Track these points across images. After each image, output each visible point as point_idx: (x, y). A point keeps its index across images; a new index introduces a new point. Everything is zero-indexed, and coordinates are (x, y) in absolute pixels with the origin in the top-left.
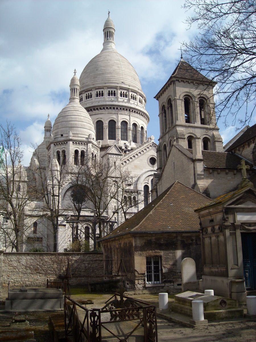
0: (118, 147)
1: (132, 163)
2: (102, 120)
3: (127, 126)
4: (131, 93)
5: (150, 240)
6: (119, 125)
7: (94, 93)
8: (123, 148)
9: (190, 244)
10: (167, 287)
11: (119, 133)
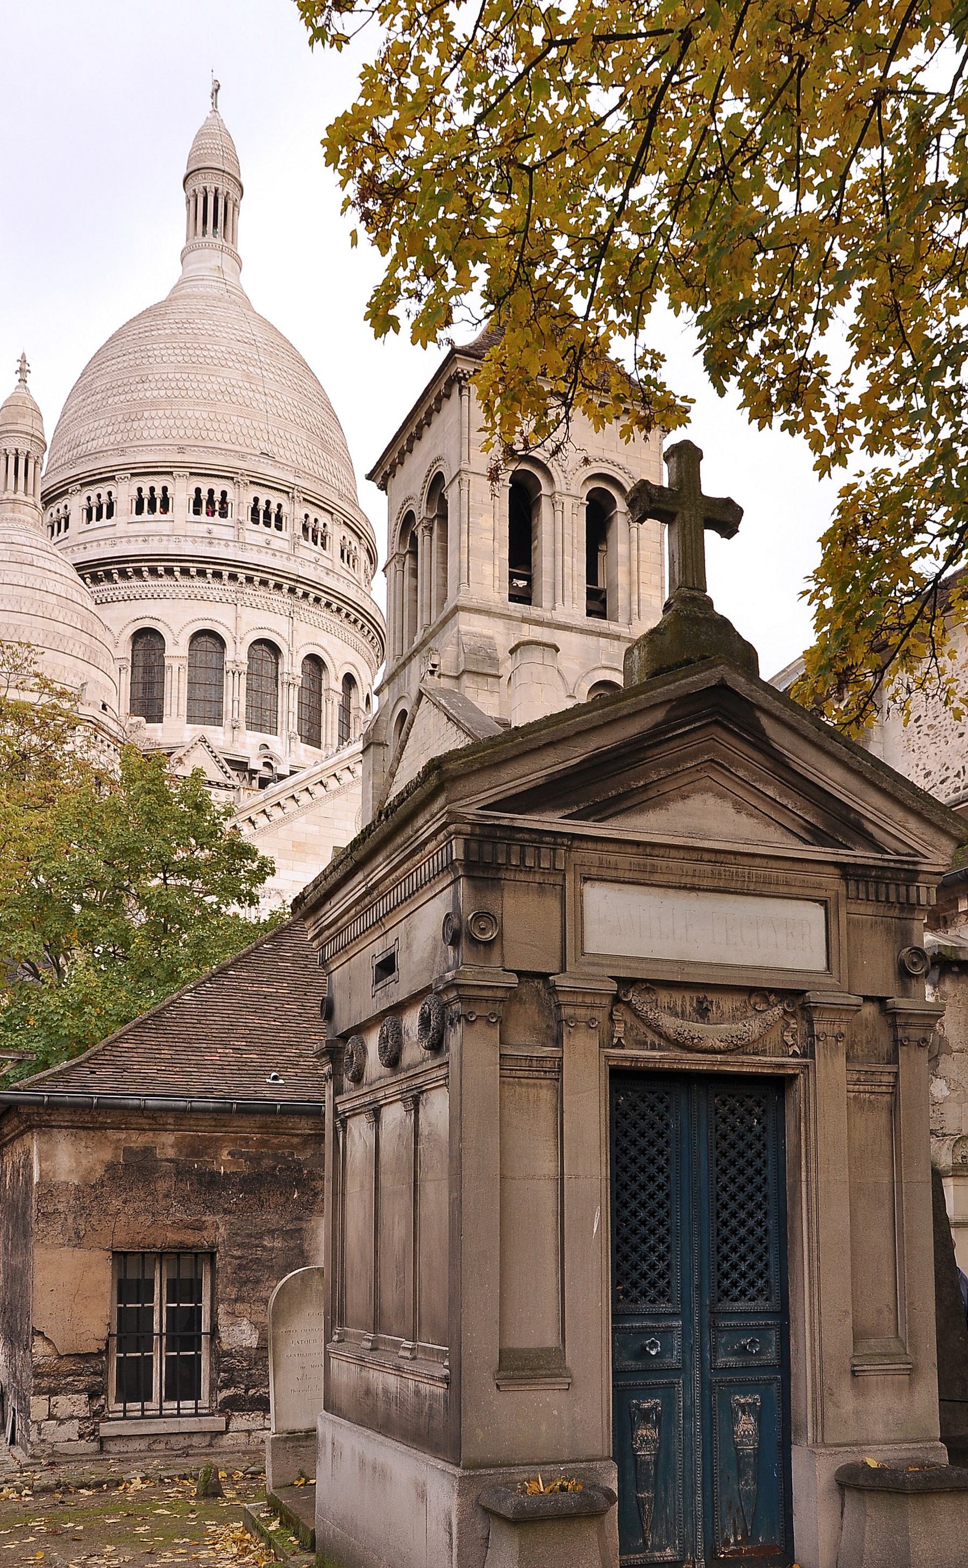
0: (221, 757)
1: (282, 832)
2: (159, 627)
3: (277, 664)
4: (301, 510)
5: (148, 1151)
7: (124, 493)
8: (256, 764)
10: (242, 1438)
11: (235, 695)
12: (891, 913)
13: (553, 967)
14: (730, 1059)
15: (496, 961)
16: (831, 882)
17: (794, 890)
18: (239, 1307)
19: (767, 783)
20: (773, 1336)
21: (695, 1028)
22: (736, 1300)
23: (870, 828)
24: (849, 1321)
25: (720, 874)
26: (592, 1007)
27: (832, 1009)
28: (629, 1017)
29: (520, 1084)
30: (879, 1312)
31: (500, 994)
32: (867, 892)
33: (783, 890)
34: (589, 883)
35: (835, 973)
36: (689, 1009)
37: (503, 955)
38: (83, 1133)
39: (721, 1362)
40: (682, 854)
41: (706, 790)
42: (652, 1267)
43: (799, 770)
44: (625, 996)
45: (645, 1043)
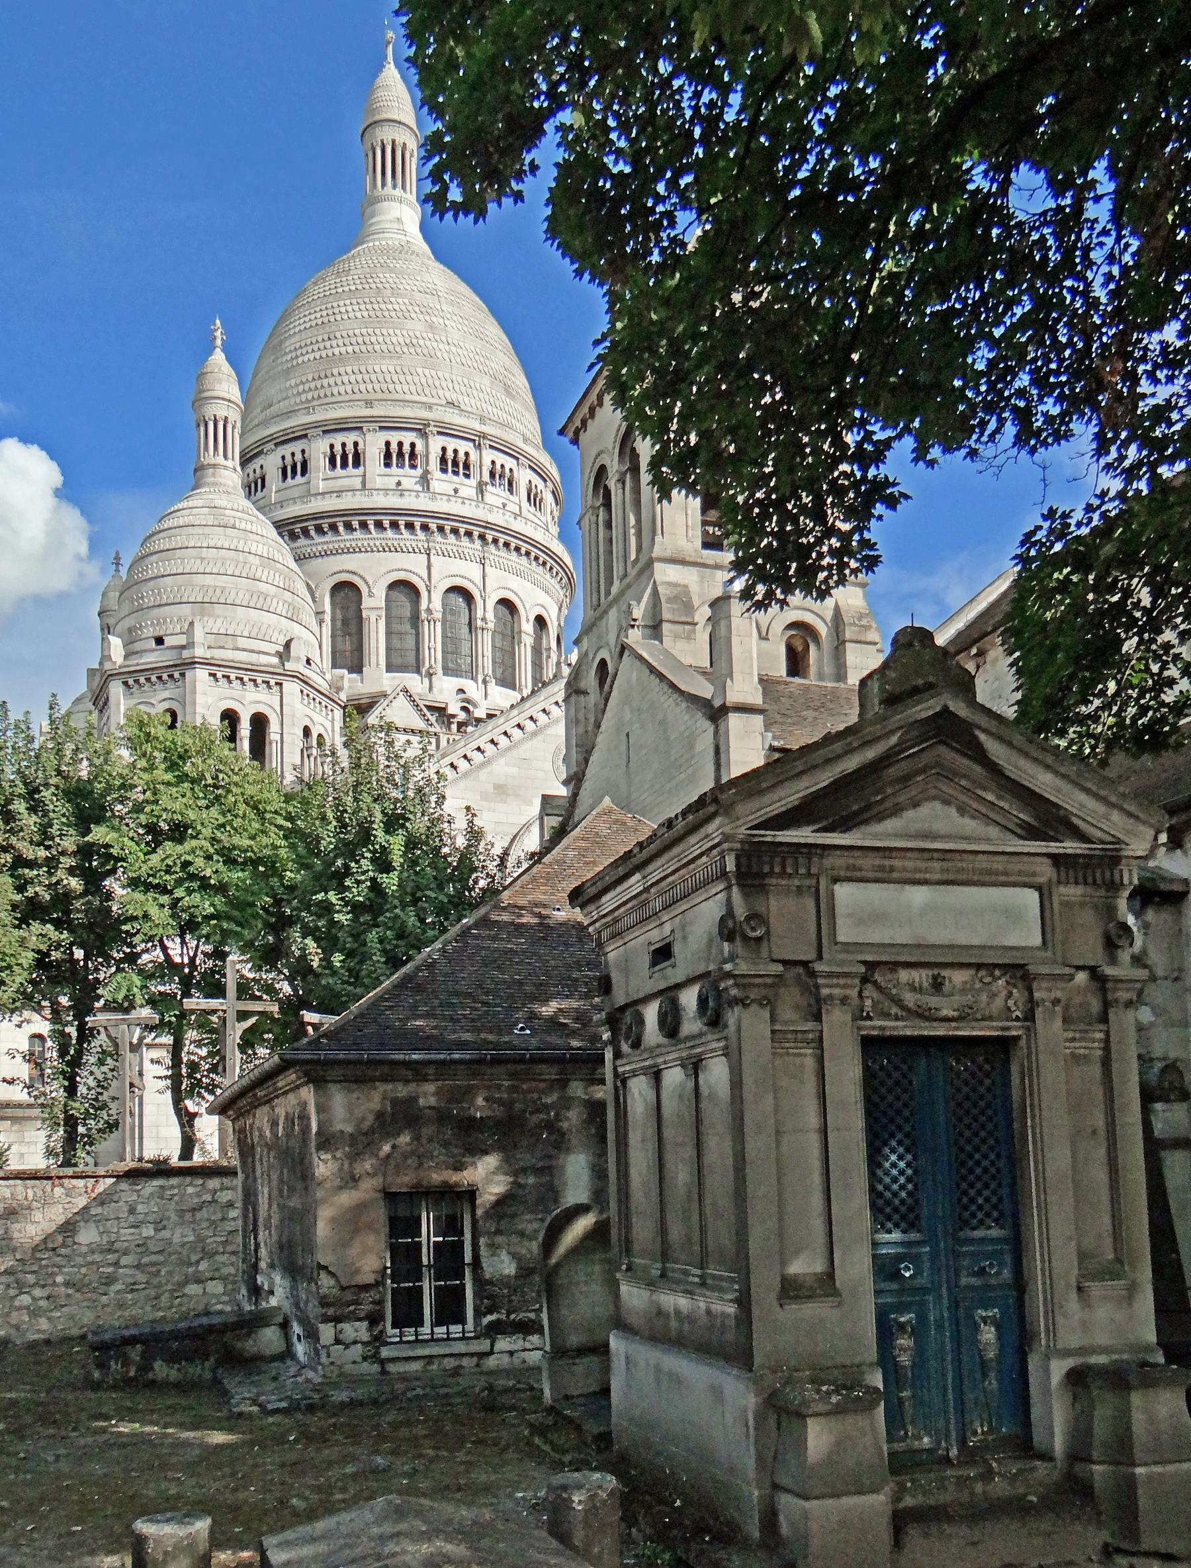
4: (489, 456)
5: (412, 1100)
6: (433, 602)
7: (319, 449)
10: (506, 1359)
13: (811, 955)
15: (765, 954)
16: (1046, 871)
17: (1012, 879)
18: (499, 1239)
19: (985, 789)
20: (1008, 1258)
21: (933, 1001)
23: (1075, 821)
26: (844, 987)
28: (875, 995)
31: (769, 981)
33: (1002, 878)
36: (925, 984)
38: (354, 1086)
39: (964, 1281)
40: (916, 855)
41: (934, 798)
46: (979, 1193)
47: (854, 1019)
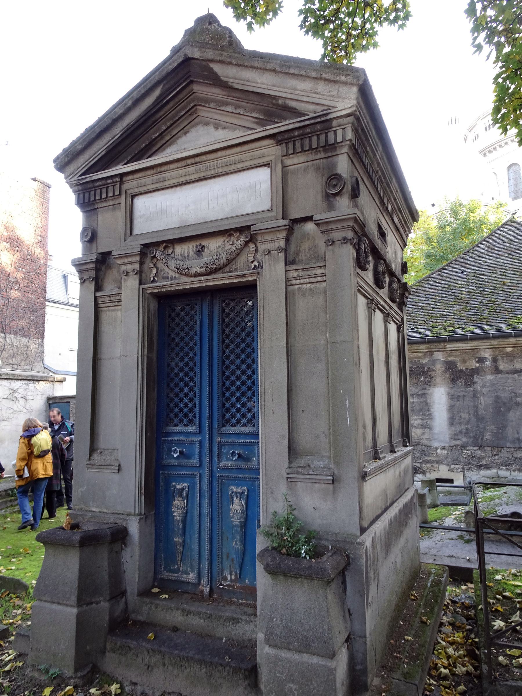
9: (475, 372)
12: (319, 156)
14: (209, 277)
16: (271, 151)
19: (226, 104)
22: (235, 426)
23: (293, 104)
24: (286, 442)
25: (200, 169)
26: (132, 263)
27: (268, 232)
29: (109, 311)
30: (317, 437)
32: (294, 149)
34: (136, 198)
35: (274, 209)
37: (97, 247)
39: (223, 463)
41: (198, 124)
42: (186, 405)
43: (240, 87)
44: (153, 253)
45: (168, 278)
46: (238, 400)
47: (141, 283)
